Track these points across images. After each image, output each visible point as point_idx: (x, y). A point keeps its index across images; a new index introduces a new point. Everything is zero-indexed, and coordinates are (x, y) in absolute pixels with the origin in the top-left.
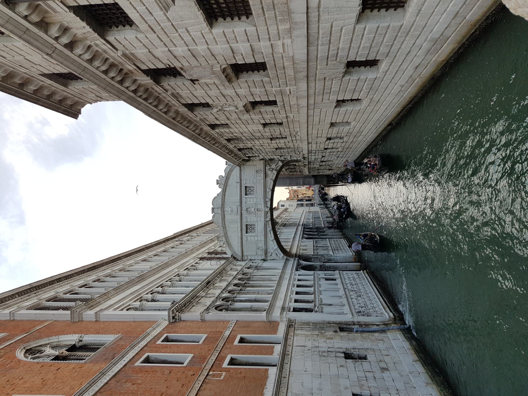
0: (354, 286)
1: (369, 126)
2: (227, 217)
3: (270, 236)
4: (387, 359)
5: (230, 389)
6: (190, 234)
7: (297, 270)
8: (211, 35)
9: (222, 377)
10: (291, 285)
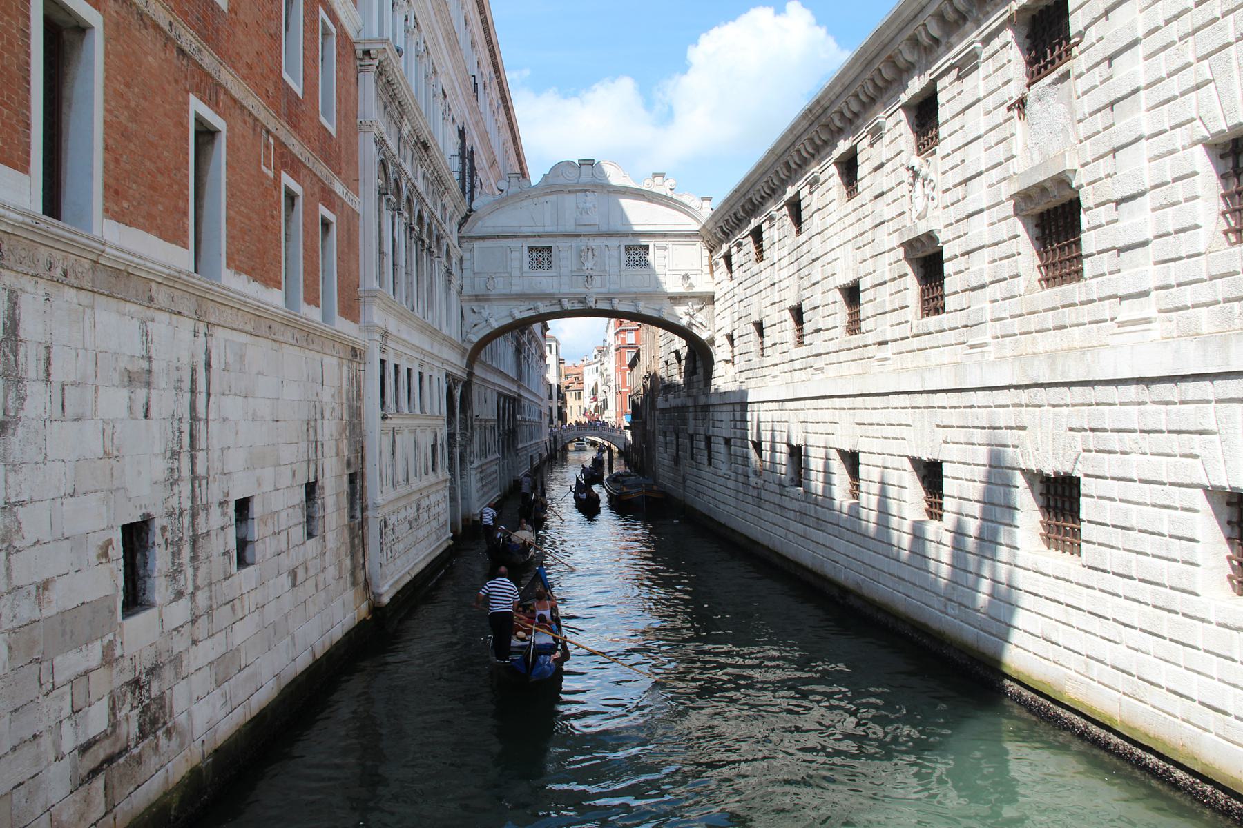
0: (426, 516)
1: (841, 545)
2: (570, 200)
3: (523, 308)
4: (310, 584)
5: (244, 187)
6: (502, 107)
7: (447, 375)
8: (1187, 141)
9: (264, 168)
10: (421, 357)
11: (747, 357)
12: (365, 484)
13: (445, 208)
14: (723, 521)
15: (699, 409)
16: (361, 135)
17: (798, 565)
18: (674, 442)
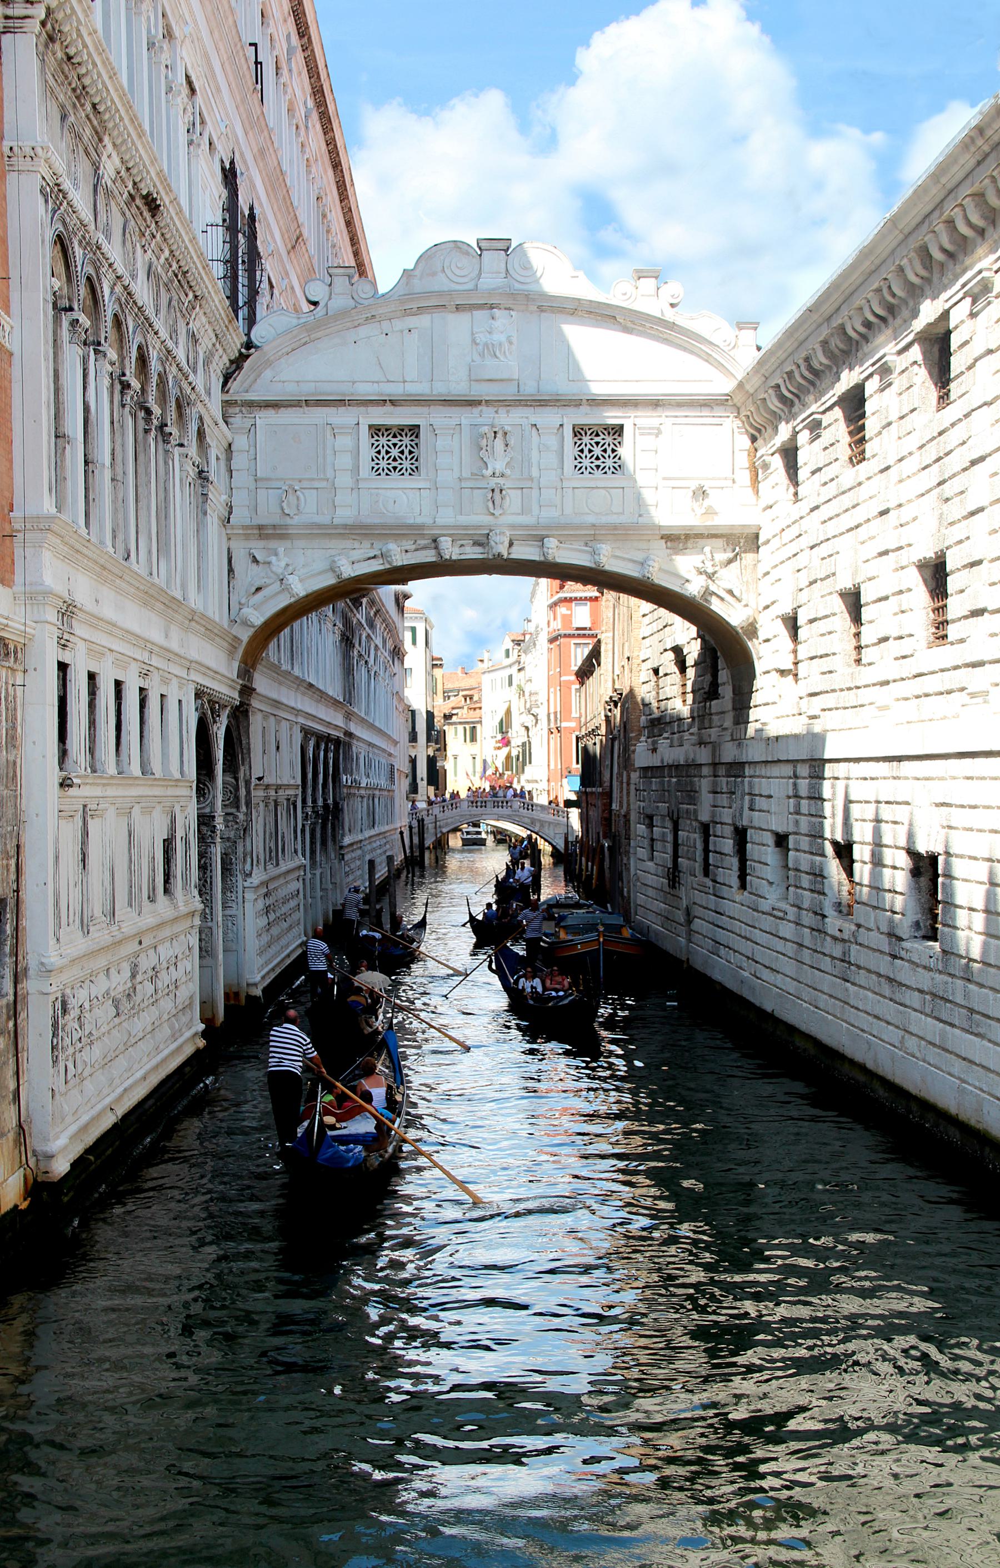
0: (150, 988)
3: (356, 555)
6: (315, 116)
7: (198, 695)
10: (145, 656)
11: (824, 664)
12: (24, 922)
13: (193, 338)
14: (768, 1007)
15: (722, 771)
16: (12, 178)
17: (927, 1106)
18: (670, 838)
